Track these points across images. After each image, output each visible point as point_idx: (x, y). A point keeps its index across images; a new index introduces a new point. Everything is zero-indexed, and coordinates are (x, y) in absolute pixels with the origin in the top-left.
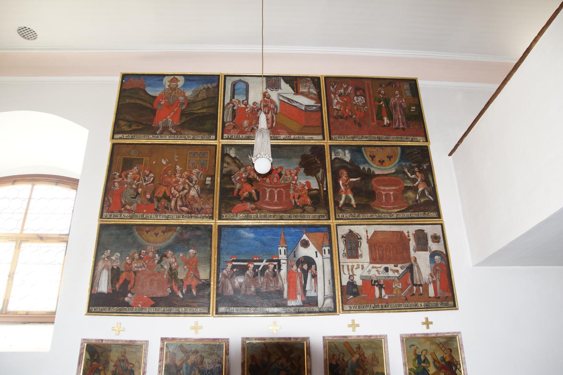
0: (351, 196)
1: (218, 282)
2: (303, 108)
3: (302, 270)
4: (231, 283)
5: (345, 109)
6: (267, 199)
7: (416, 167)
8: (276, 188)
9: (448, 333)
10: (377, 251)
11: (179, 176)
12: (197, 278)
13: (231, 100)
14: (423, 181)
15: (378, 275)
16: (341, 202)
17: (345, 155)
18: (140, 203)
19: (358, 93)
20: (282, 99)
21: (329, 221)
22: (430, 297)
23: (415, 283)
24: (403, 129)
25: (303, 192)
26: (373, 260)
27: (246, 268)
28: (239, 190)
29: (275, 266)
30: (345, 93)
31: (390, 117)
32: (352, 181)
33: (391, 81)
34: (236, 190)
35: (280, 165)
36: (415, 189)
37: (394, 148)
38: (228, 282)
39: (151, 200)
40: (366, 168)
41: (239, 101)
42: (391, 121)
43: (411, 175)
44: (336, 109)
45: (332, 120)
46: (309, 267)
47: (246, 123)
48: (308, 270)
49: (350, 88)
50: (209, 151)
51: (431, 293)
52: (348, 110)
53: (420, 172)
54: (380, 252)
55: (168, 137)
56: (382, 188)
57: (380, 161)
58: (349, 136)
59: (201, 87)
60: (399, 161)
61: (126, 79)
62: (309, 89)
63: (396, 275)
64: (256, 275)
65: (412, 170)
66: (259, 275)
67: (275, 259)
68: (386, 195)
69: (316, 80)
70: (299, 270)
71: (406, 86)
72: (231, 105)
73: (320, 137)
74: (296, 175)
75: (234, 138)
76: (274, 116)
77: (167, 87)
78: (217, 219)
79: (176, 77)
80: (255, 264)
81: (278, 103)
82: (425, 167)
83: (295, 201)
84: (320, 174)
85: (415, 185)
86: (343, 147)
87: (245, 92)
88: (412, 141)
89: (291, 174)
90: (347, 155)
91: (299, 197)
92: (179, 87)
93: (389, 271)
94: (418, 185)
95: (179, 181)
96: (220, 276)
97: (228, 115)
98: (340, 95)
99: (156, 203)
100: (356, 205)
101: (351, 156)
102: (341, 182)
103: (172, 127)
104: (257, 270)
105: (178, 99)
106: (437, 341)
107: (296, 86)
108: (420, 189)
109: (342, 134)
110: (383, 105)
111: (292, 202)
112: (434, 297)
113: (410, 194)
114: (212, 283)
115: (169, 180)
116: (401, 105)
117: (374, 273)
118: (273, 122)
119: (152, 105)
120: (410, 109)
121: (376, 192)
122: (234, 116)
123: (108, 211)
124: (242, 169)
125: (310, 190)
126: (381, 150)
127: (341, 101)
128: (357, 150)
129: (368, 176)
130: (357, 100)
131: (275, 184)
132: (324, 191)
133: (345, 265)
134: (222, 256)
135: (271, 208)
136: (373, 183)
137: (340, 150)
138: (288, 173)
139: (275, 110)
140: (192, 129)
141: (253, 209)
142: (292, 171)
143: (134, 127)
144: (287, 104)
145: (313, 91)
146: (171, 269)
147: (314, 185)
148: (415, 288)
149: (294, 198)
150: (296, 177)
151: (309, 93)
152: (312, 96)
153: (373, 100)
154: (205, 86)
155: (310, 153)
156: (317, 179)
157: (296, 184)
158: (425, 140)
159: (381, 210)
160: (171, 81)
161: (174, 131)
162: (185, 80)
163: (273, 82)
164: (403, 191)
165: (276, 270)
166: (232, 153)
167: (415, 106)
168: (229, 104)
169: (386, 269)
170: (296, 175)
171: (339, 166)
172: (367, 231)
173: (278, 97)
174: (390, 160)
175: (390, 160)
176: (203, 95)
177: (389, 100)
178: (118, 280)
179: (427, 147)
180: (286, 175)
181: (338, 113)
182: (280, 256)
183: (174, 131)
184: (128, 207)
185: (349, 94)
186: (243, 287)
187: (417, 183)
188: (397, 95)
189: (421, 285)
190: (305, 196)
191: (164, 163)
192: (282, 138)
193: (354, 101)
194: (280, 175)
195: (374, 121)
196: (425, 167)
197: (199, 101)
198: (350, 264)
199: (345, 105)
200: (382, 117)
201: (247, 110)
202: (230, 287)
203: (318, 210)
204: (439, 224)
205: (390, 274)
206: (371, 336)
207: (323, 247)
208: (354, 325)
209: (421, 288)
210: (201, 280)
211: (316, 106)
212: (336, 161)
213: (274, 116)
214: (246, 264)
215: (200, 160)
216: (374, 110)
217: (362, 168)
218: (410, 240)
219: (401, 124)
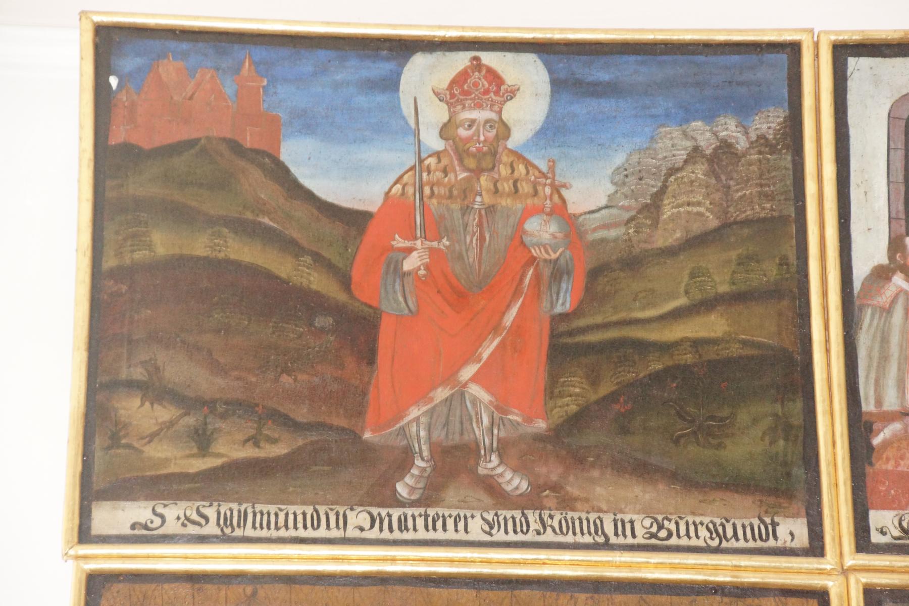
59: (673, 143)
77: (433, 141)
79: (489, 58)
92: (517, 139)
97: (884, 358)
103: (503, 449)
105: (518, 239)
140: (642, 470)
143: (231, 448)
154: (703, 134)
160: (458, 92)
161: (515, 483)
162: (558, 85)
168: (881, 274)
176: (692, 207)
183: (515, 483)
197: (670, 252)
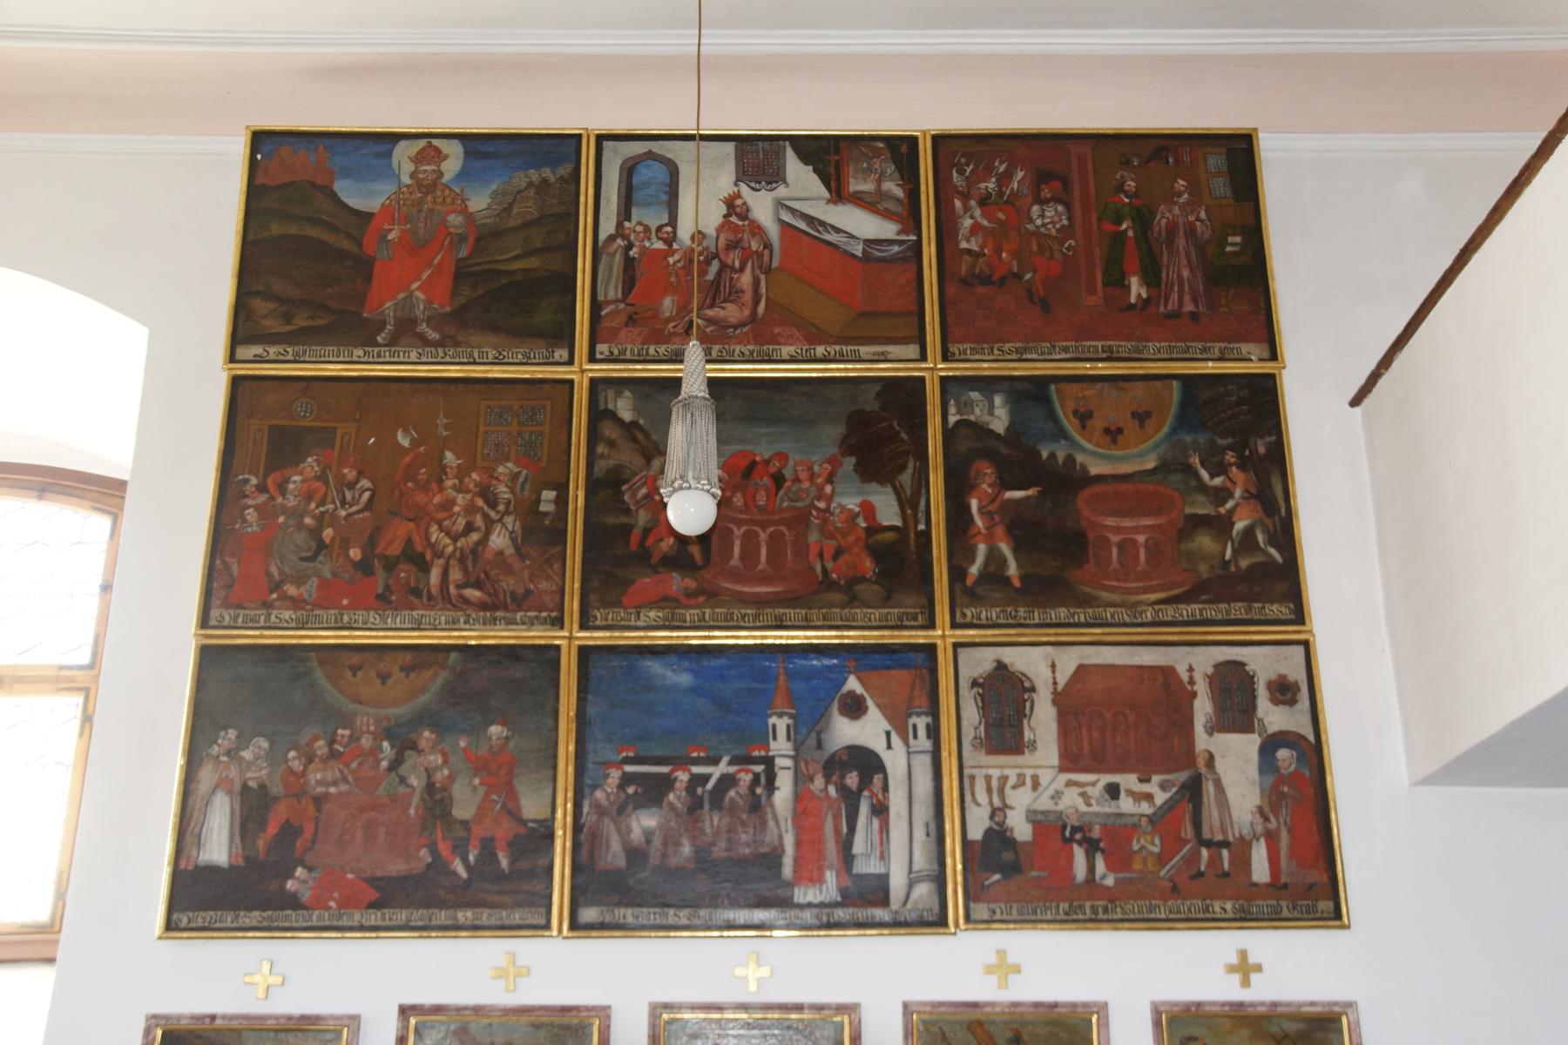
0: (1005, 548)
1: (577, 828)
2: (858, 250)
3: (843, 789)
4: (619, 830)
5: (998, 250)
6: (735, 561)
8: (764, 527)
9: (1312, 1004)
10: (1085, 732)
11: (454, 487)
12: (514, 814)
13: (619, 225)
14: (1252, 496)
15: (1083, 808)
16: (974, 570)
17: (991, 413)
18: (328, 575)
20: (787, 218)
21: (931, 633)
22: (1256, 885)
23: (1206, 835)
24: (1194, 316)
25: (851, 539)
26: (1071, 760)
27: (667, 782)
28: (647, 531)
29: (757, 777)
30: (1001, 194)
31: (1152, 277)
32: (1009, 500)
33: (1163, 142)
34: (637, 532)
35: (778, 448)
36: (1222, 525)
37: (1158, 384)
38: (609, 827)
39: (365, 567)
40: (1061, 456)
41: (647, 229)
43: (1212, 476)
44: (969, 252)
45: (952, 290)
46: (865, 782)
47: (668, 304)
48: (860, 790)
49: (1020, 175)
50: (548, 403)
51: (1260, 870)
52: (1008, 252)
53: (1242, 466)
54: (1096, 734)
55: (414, 356)
56: (1111, 521)
57: (1107, 431)
58: (1007, 346)
59: (520, 180)
60: (1174, 430)
61: (267, 148)
63: (1146, 808)
64: (695, 805)
65: (1216, 460)
66: (707, 806)
68: (1122, 546)
69: (904, 148)
70: (832, 790)
71: (1216, 161)
72: (619, 241)
73: (912, 350)
74: (830, 479)
75: (628, 356)
76: (762, 277)
77: (406, 179)
78: (576, 626)
79: (435, 142)
80: (696, 770)
81: (773, 232)
82: (1262, 450)
84: (906, 478)
85: (1222, 510)
86: (987, 384)
87: (665, 198)
88: (1221, 359)
89: (812, 476)
90: (997, 412)
91: (837, 554)
92: (447, 178)
93: (1123, 795)
94: (1232, 512)
95: (452, 503)
96: (586, 809)
97: (610, 276)
98: (984, 202)
99: (380, 574)
100: (1023, 578)
101: (1013, 415)
102: (974, 504)
103: (429, 321)
104: (699, 791)
105: (444, 224)
106: (1274, 1029)
107: (837, 168)
108: (1240, 526)
109: (985, 339)
110: (1130, 233)
111: (812, 569)
112: (1267, 885)
113: (1205, 542)
114: (559, 833)
115: (420, 498)
116: (1191, 232)
117: (1071, 802)
118: (756, 301)
119: (359, 244)
120: (1223, 243)
121: (1091, 536)
122: (629, 283)
123: (226, 604)
125: (874, 529)
126: (1114, 393)
127: (985, 223)
129: (1065, 482)
130: (1042, 216)
131: (762, 510)
132: (919, 534)
133: (980, 774)
134: (590, 746)
135: (746, 589)
137: (975, 395)
138: (803, 475)
139: (766, 258)
140: (495, 329)
141: (691, 595)
142: (816, 469)
143: (301, 321)
144: (805, 237)
145: (893, 188)
146: (430, 787)
147: (888, 512)
148: (1204, 852)
149: (821, 555)
150: (828, 489)
151: (880, 194)
152: (891, 206)
153: (1094, 216)
154: (534, 175)
155: (876, 406)
156: (898, 492)
157: (827, 510)
158: (1266, 355)
159: (1105, 595)
160: (419, 158)
161: (434, 335)
162: (467, 154)
163: (758, 156)
164: (1181, 531)
165: (759, 791)
166: (624, 408)
167: (1241, 233)
168: (612, 238)
169: (1113, 791)
170: (830, 479)
172: (1053, 666)
173: (777, 213)
174: (1142, 426)
175: (1142, 426)
176: (528, 208)
177: (1153, 214)
178: (263, 824)
179: (1272, 377)
180: (797, 480)
181: (974, 266)
182: (773, 745)
183: (434, 335)
184: (291, 590)
185: (1015, 195)
186: (657, 842)
187: (1230, 504)
188: (1180, 194)
189: (1225, 844)
190: (856, 550)
191: (404, 441)
192: (785, 356)
193: (1031, 220)
194: (778, 480)
195: (1092, 292)
196: (1262, 450)
198: (995, 773)
200: (1123, 276)
201: (671, 260)
202: (616, 845)
204: (1297, 643)
205: (1126, 805)
206: (1055, 1005)
207: (910, 716)
208: (1004, 968)
209: (1225, 853)
210: (524, 823)
211: (901, 243)
212: (963, 431)
213: (762, 277)
214: (665, 769)
215: (520, 434)
216: (1097, 252)
217: (1045, 454)
218: (1194, 695)
219: (1187, 298)
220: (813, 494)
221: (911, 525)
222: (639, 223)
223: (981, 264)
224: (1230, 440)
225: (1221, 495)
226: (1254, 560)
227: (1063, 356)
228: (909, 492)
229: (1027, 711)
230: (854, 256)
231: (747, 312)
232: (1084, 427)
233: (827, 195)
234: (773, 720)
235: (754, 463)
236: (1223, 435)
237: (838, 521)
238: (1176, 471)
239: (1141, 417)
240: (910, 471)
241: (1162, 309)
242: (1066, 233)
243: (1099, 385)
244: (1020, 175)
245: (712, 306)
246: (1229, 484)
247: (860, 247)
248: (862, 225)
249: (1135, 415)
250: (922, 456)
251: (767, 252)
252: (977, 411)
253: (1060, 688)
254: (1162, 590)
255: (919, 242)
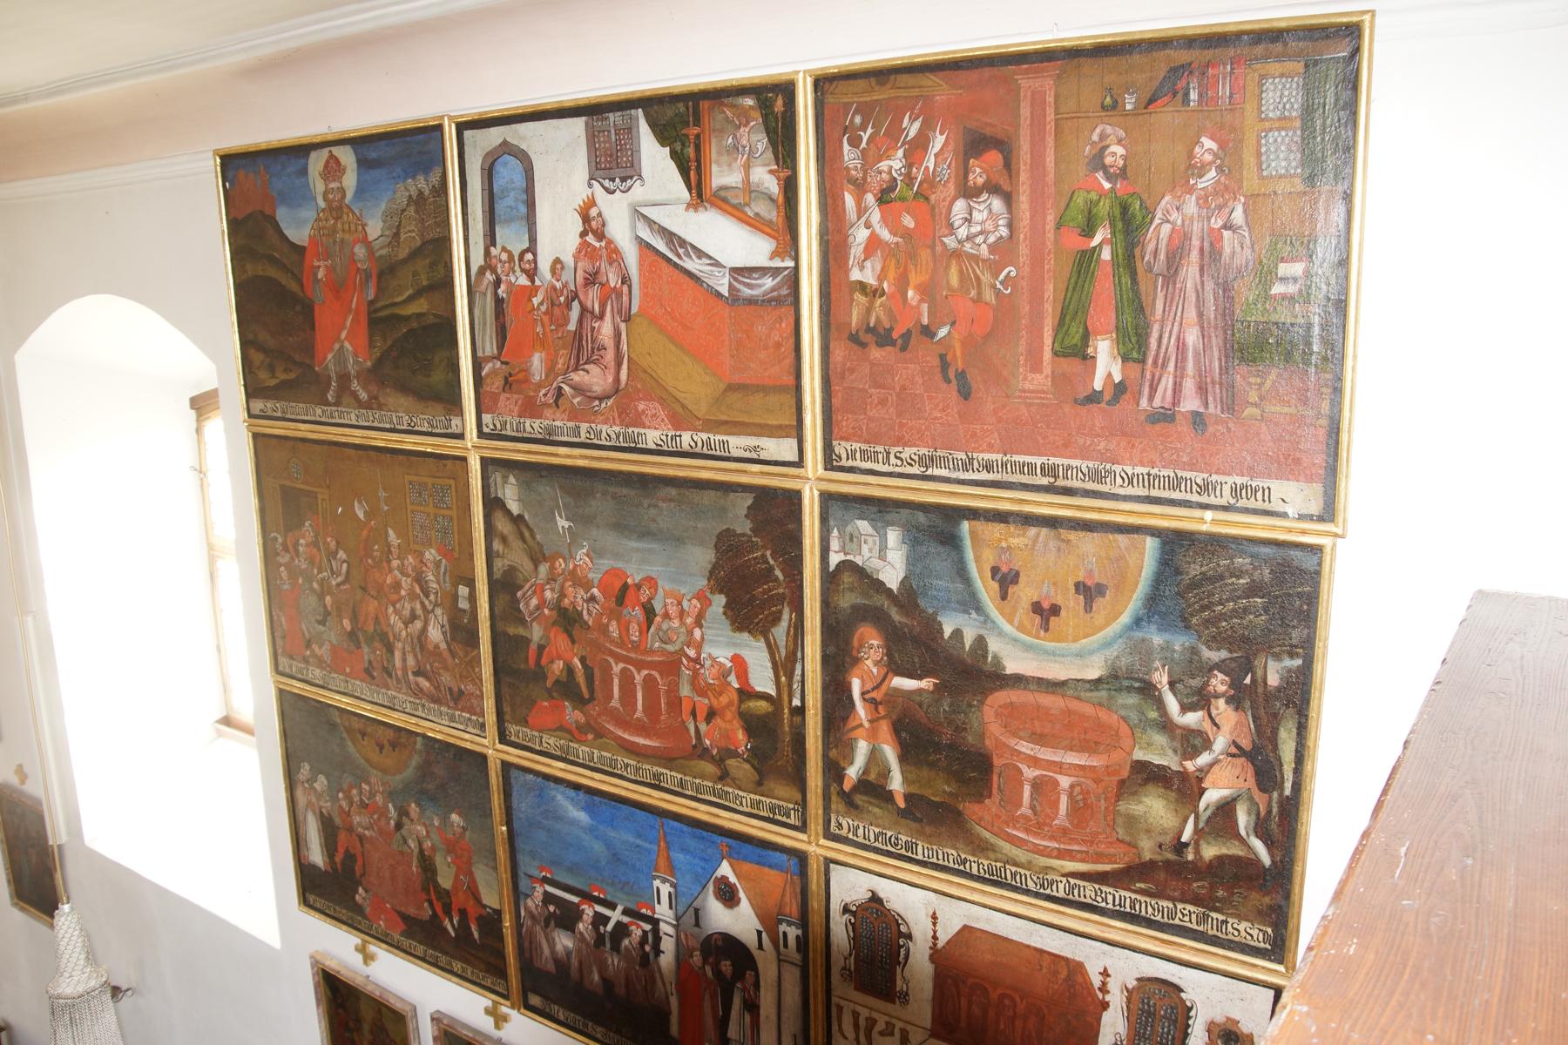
0: (890, 753)
3: (718, 973)
5: (902, 283)
7: (1219, 666)
13: (487, 253)
16: (853, 772)
17: (882, 557)
19: (977, 177)
24: (1197, 419)
25: (724, 700)
29: (645, 932)
30: (909, 179)
31: (1134, 344)
32: (897, 690)
34: (533, 646)
36: (1186, 788)
37: (1122, 539)
40: (969, 639)
42: (1135, 368)
43: (1185, 708)
44: (862, 287)
45: (838, 354)
46: (738, 975)
47: (537, 362)
50: (452, 482)
52: (918, 288)
53: (1235, 701)
56: (1025, 747)
57: (1037, 608)
58: (908, 452)
60: (1137, 622)
62: (747, 168)
65: (1196, 683)
67: (644, 911)
68: (1037, 785)
69: (779, 105)
76: (623, 326)
77: (322, 204)
82: (1273, 680)
83: (697, 728)
84: (780, 632)
85: (1190, 766)
87: (523, 209)
89: (682, 614)
91: (711, 715)
98: (883, 198)
100: (908, 797)
101: (912, 561)
108: (1212, 796)
110: (1106, 254)
111: (687, 730)
113: (1155, 808)
118: (619, 365)
121: (997, 762)
124: (543, 569)
125: (746, 693)
127: (885, 235)
128: (938, 528)
129: (972, 675)
130: (968, 221)
131: (636, 647)
133: (848, 1008)
135: (626, 736)
136: (988, 713)
137: (864, 526)
138: (673, 611)
142: (685, 604)
145: (766, 179)
146: (421, 851)
147: (763, 679)
149: (694, 714)
151: (749, 188)
153: (1051, 218)
156: (772, 649)
159: (1006, 847)
164: (1122, 782)
165: (647, 948)
168: (482, 271)
171: (856, 604)
173: (634, 228)
174: (1088, 607)
175: (1088, 607)
177: (1149, 213)
178: (336, 850)
180: (666, 616)
181: (869, 311)
183: (363, 396)
185: (930, 182)
187: (1204, 759)
188: (1201, 171)
190: (729, 715)
193: (951, 229)
194: (650, 613)
195: (1036, 367)
196: (1273, 680)
197: (405, 261)
198: (864, 1013)
199: (900, 257)
200: (1086, 337)
203: (770, 784)
210: (484, 906)
211: (775, 272)
213: (623, 326)
214: (576, 899)
217: (948, 631)
218: (1105, 1006)
219: (1189, 385)
220: (683, 638)
221: (785, 697)
222: (504, 249)
223: (879, 314)
224: (1224, 654)
225: (1193, 742)
226: (1225, 851)
227: (984, 476)
228: (783, 652)
229: (901, 958)
230: (719, 295)
231: (610, 379)
232: (1004, 597)
233: (686, 195)
234: (657, 883)
235: (625, 587)
236: (1215, 641)
237: (709, 675)
238: (1129, 689)
239: (1089, 592)
240: (784, 624)
241: (1144, 403)
242: (1004, 250)
243: (1033, 531)
244: (938, 141)
245: (576, 369)
246: (1207, 726)
247: (726, 281)
248: (728, 244)
249: (1081, 588)
250: (798, 607)
251: (625, 288)
252: (865, 548)
253: (940, 944)
254: (1083, 861)
255: (796, 269)
